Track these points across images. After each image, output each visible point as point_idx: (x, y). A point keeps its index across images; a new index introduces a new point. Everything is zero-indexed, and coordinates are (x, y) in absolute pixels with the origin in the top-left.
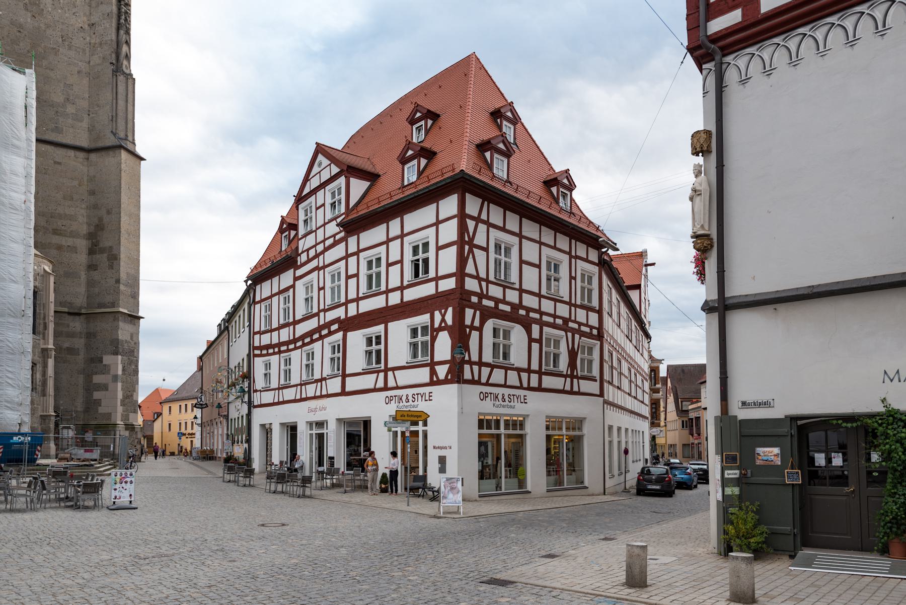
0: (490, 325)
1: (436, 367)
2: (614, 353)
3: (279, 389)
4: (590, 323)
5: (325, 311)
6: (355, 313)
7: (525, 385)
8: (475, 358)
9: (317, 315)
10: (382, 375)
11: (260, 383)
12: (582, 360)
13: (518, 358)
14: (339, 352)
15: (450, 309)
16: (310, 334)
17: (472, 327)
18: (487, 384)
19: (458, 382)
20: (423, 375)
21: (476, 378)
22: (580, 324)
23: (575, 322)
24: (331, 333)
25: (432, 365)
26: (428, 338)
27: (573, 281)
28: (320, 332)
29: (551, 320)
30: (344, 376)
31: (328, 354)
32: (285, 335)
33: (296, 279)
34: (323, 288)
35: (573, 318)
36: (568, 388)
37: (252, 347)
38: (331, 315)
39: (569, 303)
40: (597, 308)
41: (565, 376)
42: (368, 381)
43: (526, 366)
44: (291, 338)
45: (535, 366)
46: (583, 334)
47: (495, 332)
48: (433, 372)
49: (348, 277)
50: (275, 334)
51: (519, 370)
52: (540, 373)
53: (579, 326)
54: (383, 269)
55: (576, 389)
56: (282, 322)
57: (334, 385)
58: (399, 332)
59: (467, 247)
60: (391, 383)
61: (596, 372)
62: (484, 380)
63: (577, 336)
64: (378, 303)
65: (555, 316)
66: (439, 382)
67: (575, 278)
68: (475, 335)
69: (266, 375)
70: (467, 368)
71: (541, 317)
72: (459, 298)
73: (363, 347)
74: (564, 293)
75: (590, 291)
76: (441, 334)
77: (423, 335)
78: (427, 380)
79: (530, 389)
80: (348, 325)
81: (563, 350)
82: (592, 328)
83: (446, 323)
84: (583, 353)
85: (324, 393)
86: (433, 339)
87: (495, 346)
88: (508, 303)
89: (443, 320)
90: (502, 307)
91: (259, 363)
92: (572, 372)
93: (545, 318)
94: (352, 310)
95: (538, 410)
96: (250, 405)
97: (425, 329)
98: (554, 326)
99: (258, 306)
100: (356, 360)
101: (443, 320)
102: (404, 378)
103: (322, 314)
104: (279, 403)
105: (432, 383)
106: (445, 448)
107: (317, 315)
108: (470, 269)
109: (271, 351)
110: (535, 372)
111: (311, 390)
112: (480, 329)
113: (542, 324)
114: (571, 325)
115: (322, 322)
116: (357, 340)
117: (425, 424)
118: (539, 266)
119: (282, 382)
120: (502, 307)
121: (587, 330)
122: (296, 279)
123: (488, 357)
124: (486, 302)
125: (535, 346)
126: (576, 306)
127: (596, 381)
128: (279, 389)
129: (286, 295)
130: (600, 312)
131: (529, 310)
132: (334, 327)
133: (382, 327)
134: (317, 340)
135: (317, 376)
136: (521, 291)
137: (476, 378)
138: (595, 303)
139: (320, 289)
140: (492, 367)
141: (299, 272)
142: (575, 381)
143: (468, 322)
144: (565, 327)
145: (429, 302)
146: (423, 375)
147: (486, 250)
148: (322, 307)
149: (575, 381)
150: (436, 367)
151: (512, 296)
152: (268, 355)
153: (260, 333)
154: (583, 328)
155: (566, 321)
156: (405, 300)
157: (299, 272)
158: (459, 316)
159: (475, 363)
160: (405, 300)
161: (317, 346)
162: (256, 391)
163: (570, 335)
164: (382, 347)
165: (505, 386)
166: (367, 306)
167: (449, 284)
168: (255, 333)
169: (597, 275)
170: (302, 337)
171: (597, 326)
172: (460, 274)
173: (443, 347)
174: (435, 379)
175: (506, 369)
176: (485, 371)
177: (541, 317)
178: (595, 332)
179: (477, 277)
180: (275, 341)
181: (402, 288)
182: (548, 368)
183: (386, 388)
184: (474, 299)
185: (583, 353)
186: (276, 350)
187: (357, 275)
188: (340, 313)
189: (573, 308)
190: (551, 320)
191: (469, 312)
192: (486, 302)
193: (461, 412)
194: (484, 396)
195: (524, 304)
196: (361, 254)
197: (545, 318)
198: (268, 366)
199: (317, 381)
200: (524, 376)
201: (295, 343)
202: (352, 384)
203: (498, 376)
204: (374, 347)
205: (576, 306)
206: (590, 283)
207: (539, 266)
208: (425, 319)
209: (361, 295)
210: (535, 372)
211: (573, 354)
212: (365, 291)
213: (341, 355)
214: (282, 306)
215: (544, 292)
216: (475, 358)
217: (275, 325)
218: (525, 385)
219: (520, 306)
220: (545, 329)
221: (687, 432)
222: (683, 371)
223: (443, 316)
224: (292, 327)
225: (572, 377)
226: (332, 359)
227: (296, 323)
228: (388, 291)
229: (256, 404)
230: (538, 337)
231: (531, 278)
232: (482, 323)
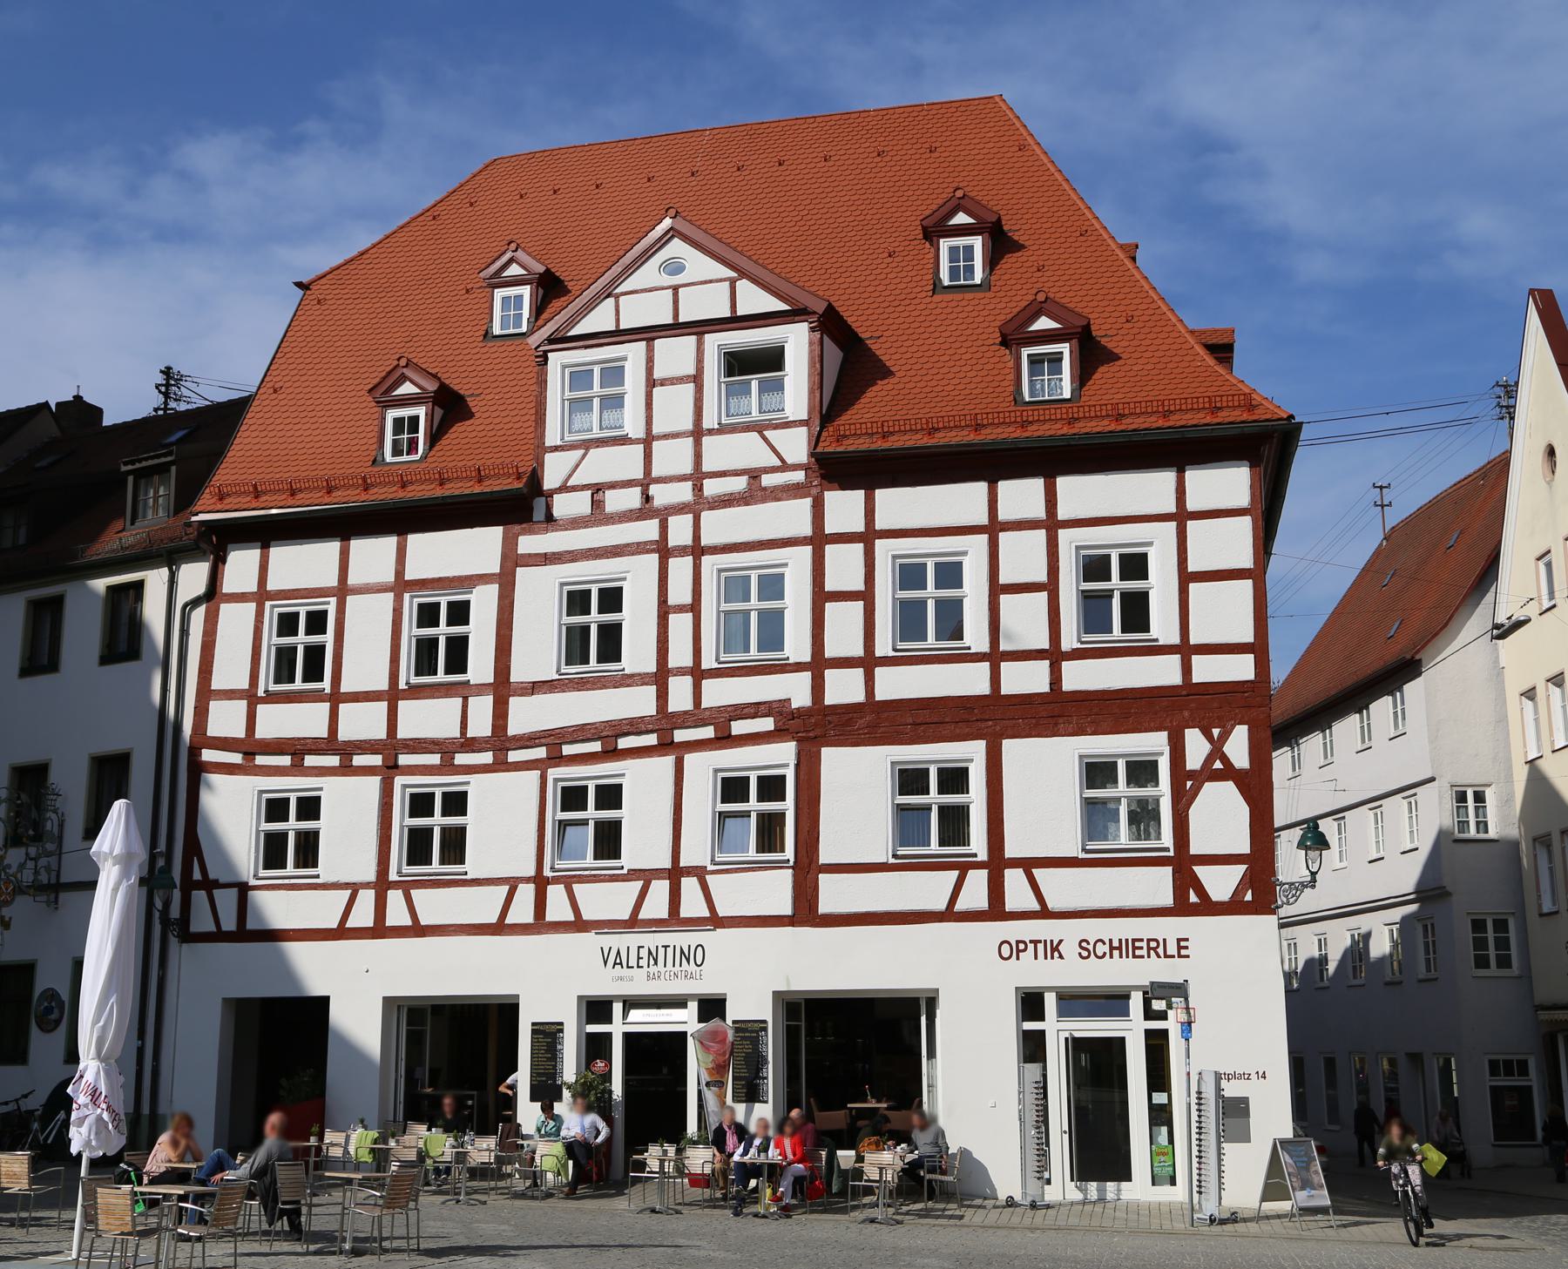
24: (725, 739)
25: (1183, 864)
30: (807, 871)
42: (931, 890)
48: (1185, 880)
64: (971, 681)
66: (1209, 907)
76: (1209, 788)
78: (1167, 899)
80: (816, 728)
89: (1217, 752)
101: (1217, 752)
102: (1061, 887)
105: (1180, 908)
122: (512, 561)
132: (767, 724)
146: (1157, 885)
157: (528, 544)
170: (554, 742)
173: (1220, 820)
174: (1193, 898)
183: (996, 910)
188: (796, 690)
199: (646, 876)
208: (1153, 743)
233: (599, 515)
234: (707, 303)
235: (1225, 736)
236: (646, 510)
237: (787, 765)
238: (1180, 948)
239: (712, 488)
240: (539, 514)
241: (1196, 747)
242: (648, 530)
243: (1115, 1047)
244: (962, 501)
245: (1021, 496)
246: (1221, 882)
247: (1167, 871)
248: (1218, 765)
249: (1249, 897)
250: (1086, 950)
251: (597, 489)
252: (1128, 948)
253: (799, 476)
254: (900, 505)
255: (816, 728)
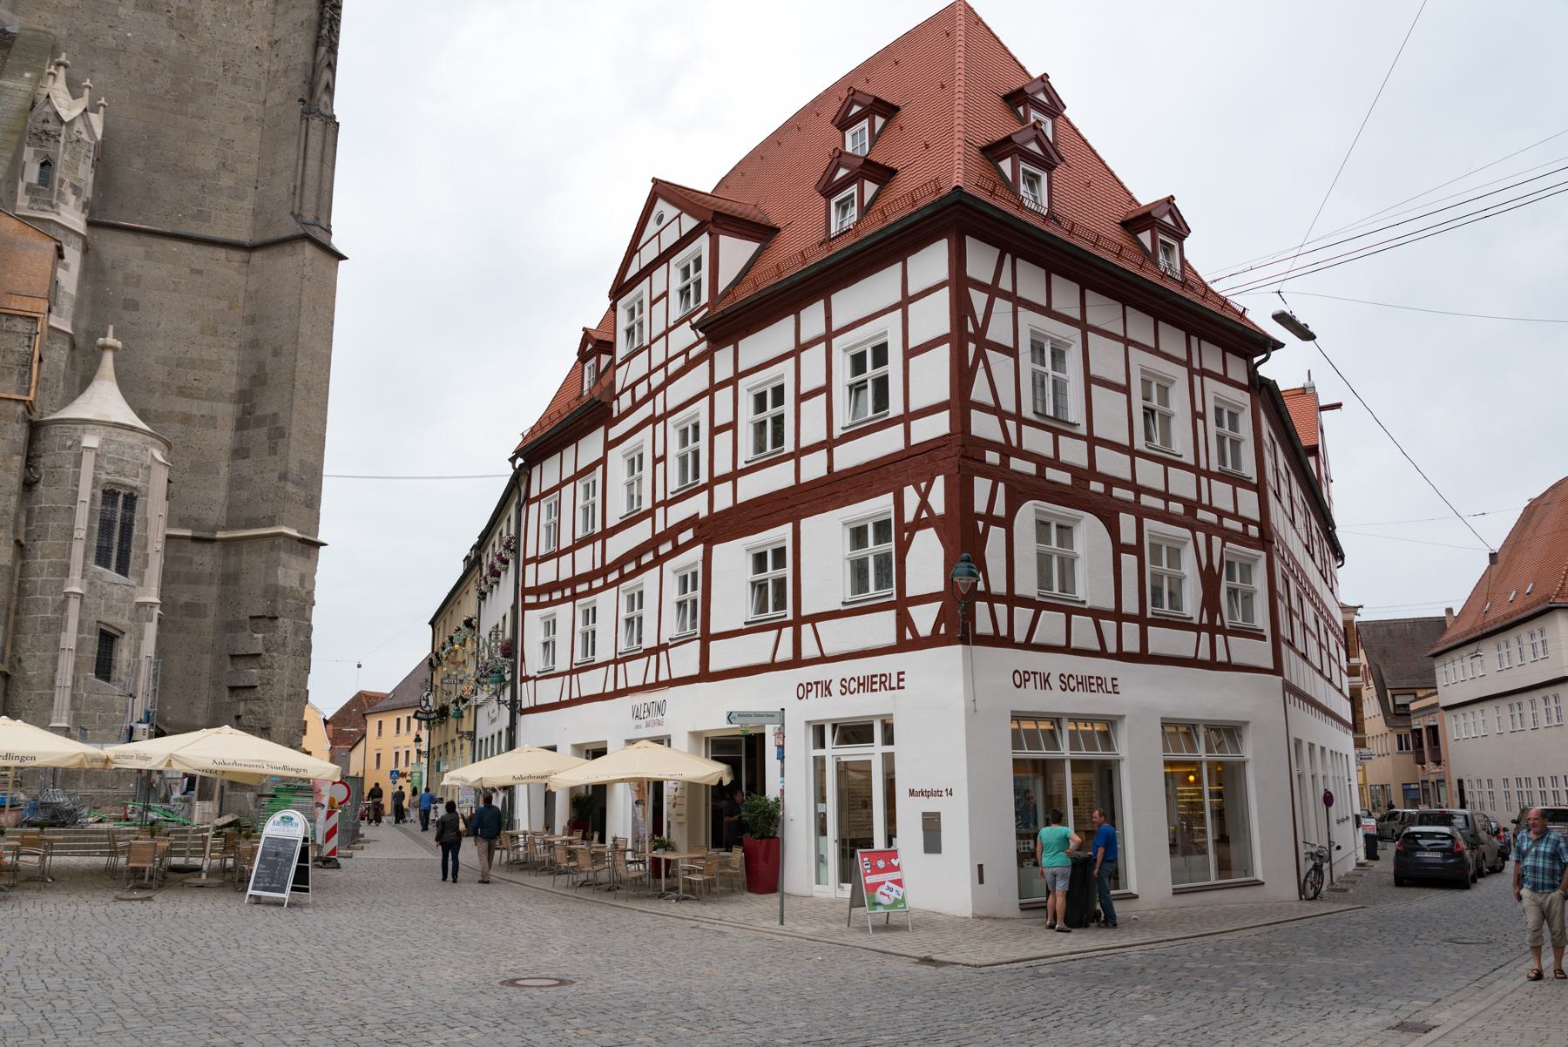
0: (1028, 513)
1: (911, 610)
2: (1291, 581)
3: (571, 672)
4: (1241, 513)
5: (667, 504)
6: (729, 504)
7: (1112, 647)
8: (998, 586)
9: (650, 513)
10: (788, 632)
11: (534, 661)
12: (1232, 592)
13: (1091, 587)
14: (694, 588)
15: (939, 482)
16: (635, 554)
17: (990, 519)
18: (1028, 645)
19: (964, 641)
20: (882, 627)
21: (1003, 631)
22: (1221, 514)
23: (1210, 508)
24: (678, 550)
25: (902, 605)
26: (891, 546)
27: (1200, 422)
28: (656, 550)
29: (1158, 504)
30: (706, 638)
31: (672, 594)
32: (585, 560)
33: (609, 445)
34: (664, 458)
35: (1205, 501)
36: (1204, 654)
37: (521, 590)
38: (679, 513)
39: (1195, 469)
40: (1255, 481)
41: (1198, 628)
42: (758, 648)
43: (1110, 605)
44: (598, 565)
45: (1130, 605)
46: (1228, 536)
47: (1042, 526)
48: (904, 622)
49: (715, 431)
50: (566, 560)
51: (1097, 614)
52: (1142, 621)
53: (1220, 518)
54: (788, 408)
55: (1221, 656)
56: (579, 535)
57: (685, 660)
58: (825, 540)
59: (972, 347)
60: (809, 650)
61: (1261, 620)
62: (1020, 636)
63: (1216, 541)
64: (778, 478)
65: (1166, 496)
66: (919, 643)
67: (1203, 416)
68: (996, 535)
69: (546, 644)
70: (981, 607)
71: (1137, 497)
72: (960, 456)
73: (748, 574)
74: (1181, 445)
75: (1236, 444)
76: (919, 535)
77: (878, 541)
79: (1121, 656)
80: (713, 530)
81: (1189, 567)
82: (1246, 522)
83: (930, 511)
84: (1231, 577)
85: (664, 676)
86: (903, 548)
87: (1043, 560)
88: (1064, 467)
89: (924, 505)
90: (1052, 474)
91: (533, 621)
92: (1212, 618)
93: (1146, 500)
94: (724, 498)
95: (1146, 699)
96: (516, 709)
97: (882, 529)
98: (1165, 517)
99: (534, 508)
100: (732, 601)
101: (924, 505)
102: (837, 636)
103: (660, 512)
104: (571, 703)
105: (902, 646)
106: (938, 793)
107: (650, 513)
108: (980, 391)
109: (557, 595)
110: (1130, 618)
111: (635, 672)
112: (1007, 523)
113: (1141, 513)
114: (1202, 515)
115: (660, 528)
116: (733, 560)
117: (889, 739)
118: (1126, 390)
119: (578, 658)
120: (1052, 474)
121: (1237, 526)
123: (1027, 585)
124: (1016, 464)
125: (1129, 561)
126: (1209, 475)
127: (1263, 638)
128: (571, 672)
129: (588, 479)
130: (1260, 488)
131: (1110, 482)
133: (789, 526)
134: (650, 566)
135: (649, 641)
136: (1092, 441)
137: (1003, 631)
138: (1249, 469)
139: (656, 461)
140: (1038, 606)
141: (615, 433)
142: (1219, 638)
143: (980, 506)
144: (1189, 519)
145: (891, 468)
146: (882, 627)
147: (1013, 352)
148: (660, 497)
149: (1219, 638)
150: (911, 610)
151: (1074, 452)
152: (552, 603)
153: (538, 560)
154: (1228, 523)
155: (1191, 506)
156: (837, 468)
157: (615, 433)
158: (960, 495)
159: (999, 598)
160: (837, 468)
161: (649, 579)
162: (526, 679)
163: (1201, 536)
164: (788, 572)
165: (1067, 649)
166: (753, 487)
167: (937, 426)
168: (527, 562)
169: (1248, 410)
170: (620, 563)
171: (1257, 518)
172: (960, 403)
173: (927, 563)
174: (909, 636)
175: (1069, 612)
176: (1023, 615)
177: (1137, 497)
178: (1253, 531)
179: (996, 410)
180: (566, 574)
181: (829, 444)
182: (1158, 610)
183: (797, 662)
184: (992, 457)
185: (1231, 577)
186: (568, 592)
187: (733, 426)
188: (697, 506)
189: (1204, 480)
190: (1158, 504)
191: (982, 486)
192: (1016, 464)
193: (973, 711)
194: (1022, 678)
195: (1100, 467)
196: (741, 382)
197: (1146, 500)
198: (550, 626)
199: (648, 652)
200: (1109, 626)
201: (605, 577)
202: (723, 655)
203: (1051, 627)
204: (771, 573)
205: (1209, 475)
206: (1234, 426)
207: (1126, 390)
208: (881, 505)
209: (741, 465)
210: (1130, 618)
211: (1210, 580)
212: (751, 456)
213: (699, 594)
214: (580, 502)
215: (1140, 444)
216: (998, 586)
217: (566, 542)
218: (1112, 647)
219: (1091, 472)
220: (1149, 524)
221: (1409, 758)
222: (1390, 632)
223: (924, 496)
224: (599, 544)
225: (1213, 629)
226: (681, 605)
227: (607, 533)
228: (799, 453)
229: (525, 705)
230: (1134, 542)
231: (1111, 416)
232: (1012, 508)
233: (636, 406)
234: (670, 237)
235: (929, 488)
236: (651, 395)
237: (695, 564)
238: (900, 680)
239: (673, 367)
240: (615, 414)
241: (911, 498)
242: (645, 411)
243: (865, 768)
244: (778, 336)
245: (812, 320)
246: (925, 618)
247: (892, 614)
248: (924, 515)
249: (942, 631)
250: (845, 690)
251: (633, 386)
252: (867, 684)
253: (703, 346)
254: (755, 347)
255: (713, 530)
